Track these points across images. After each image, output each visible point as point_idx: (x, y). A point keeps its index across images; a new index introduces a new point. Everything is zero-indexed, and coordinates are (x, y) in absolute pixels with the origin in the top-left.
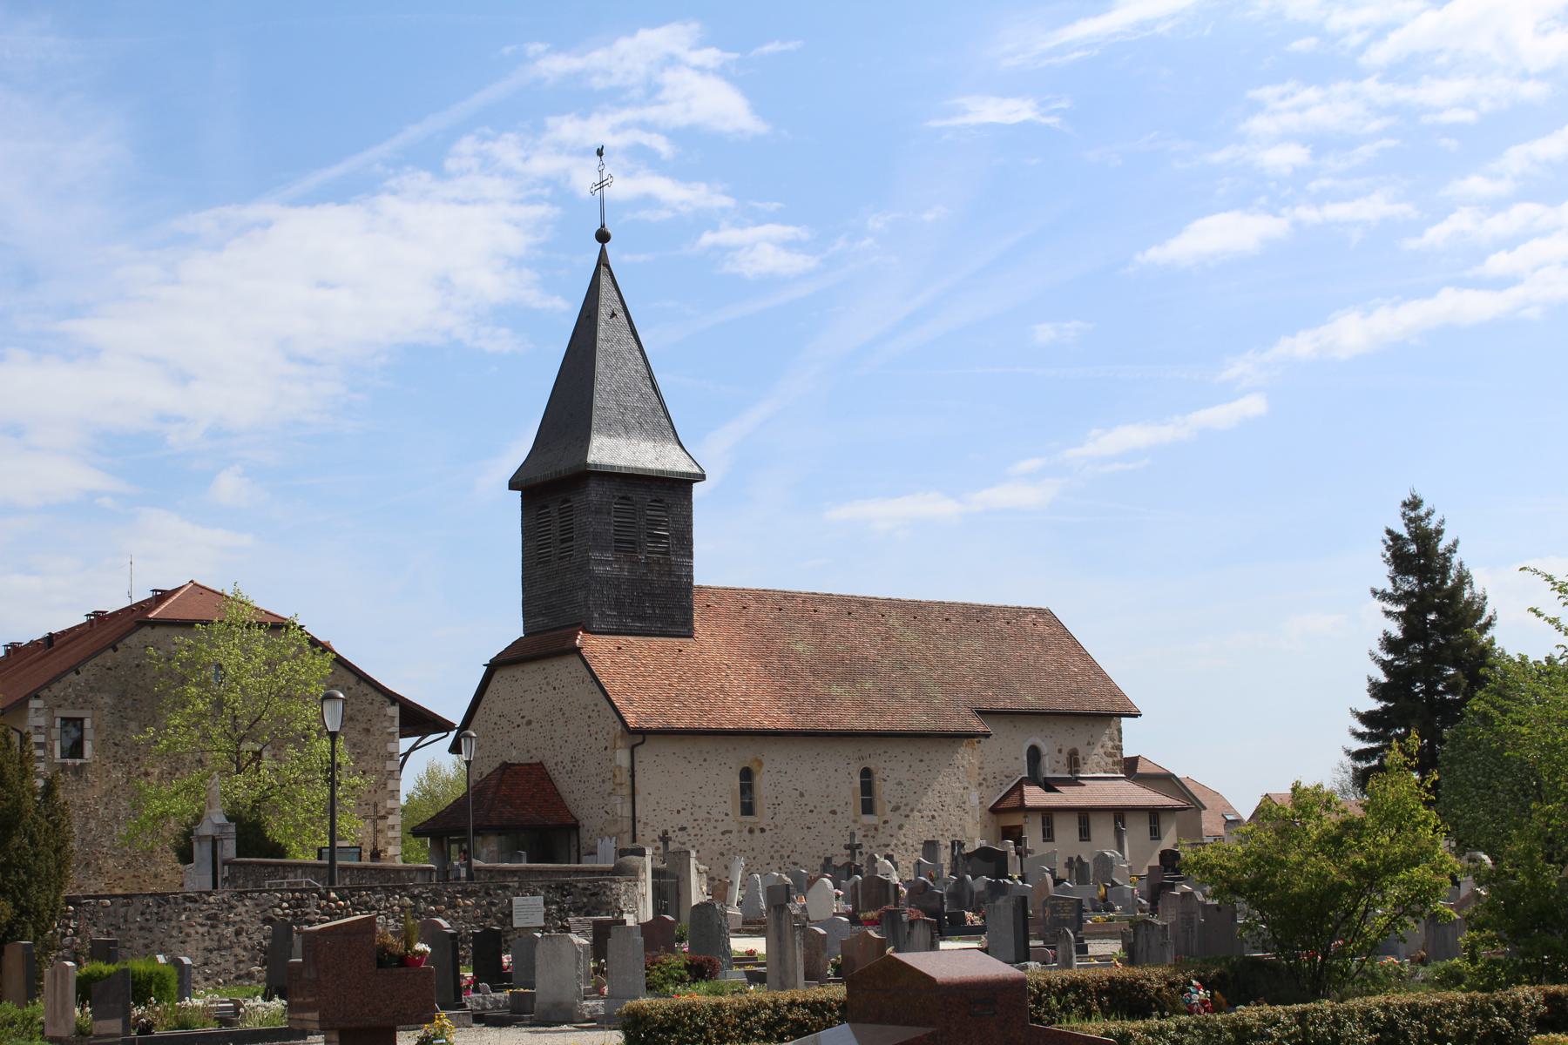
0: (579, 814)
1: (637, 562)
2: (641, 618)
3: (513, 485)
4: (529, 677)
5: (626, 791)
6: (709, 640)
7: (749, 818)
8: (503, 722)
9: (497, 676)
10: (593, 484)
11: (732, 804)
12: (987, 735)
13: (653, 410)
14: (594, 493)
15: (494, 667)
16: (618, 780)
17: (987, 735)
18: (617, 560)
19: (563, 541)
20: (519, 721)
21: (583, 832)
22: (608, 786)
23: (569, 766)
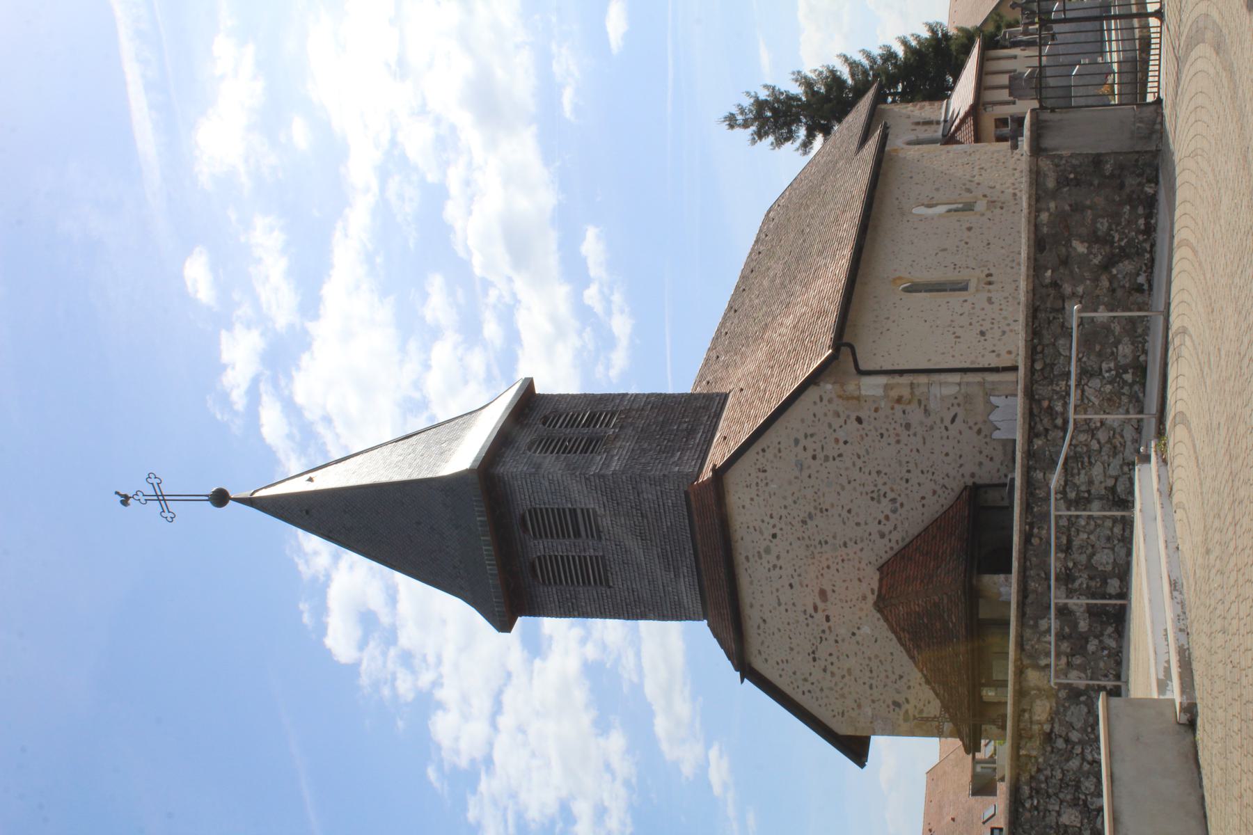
0: (956, 485)
1: (617, 437)
2: (691, 433)
3: (504, 625)
4: (760, 588)
5: (923, 379)
6: (733, 382)
7: (972, 285)
8: (822, 653)
9: (758, 664)
10: (500, 470)
11: (955, 299)
12: (886, 128)
13: (424, 404)
14: (513, 467)
15: (747, 670)
16: (906, 392)
17: (886, 128)
18: (608, 451)
19: (577, 534)
20: (820, 616)
21: (984, 477)
22: (916, 415)
23: (885, 505)
